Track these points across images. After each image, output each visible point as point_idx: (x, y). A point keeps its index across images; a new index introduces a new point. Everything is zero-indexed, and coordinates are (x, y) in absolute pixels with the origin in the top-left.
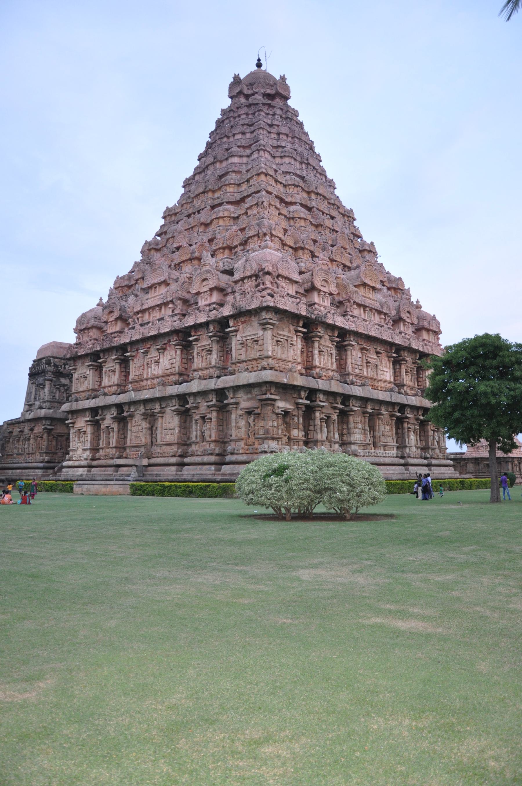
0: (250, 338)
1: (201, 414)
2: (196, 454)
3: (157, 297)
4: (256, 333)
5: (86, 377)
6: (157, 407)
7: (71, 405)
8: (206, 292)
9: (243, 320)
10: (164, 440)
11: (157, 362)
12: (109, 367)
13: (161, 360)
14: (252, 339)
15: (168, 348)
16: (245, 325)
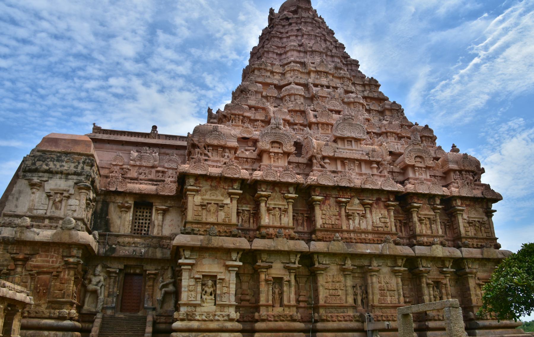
0: (477, 220)
1: (434, 278)
2: (436, 318)
3: (354, 152)
4: (482, 217)
5: (223, 207)
6: (375, 263)
7: (209, 240)
8: (421, 167)
9: (467, 203)
10: (383, 302)
11: (364, 216)
12: (275, 204)
13: (368, 215)
14: (478, 221)
15: (375, 205)
16: (469, 209)
